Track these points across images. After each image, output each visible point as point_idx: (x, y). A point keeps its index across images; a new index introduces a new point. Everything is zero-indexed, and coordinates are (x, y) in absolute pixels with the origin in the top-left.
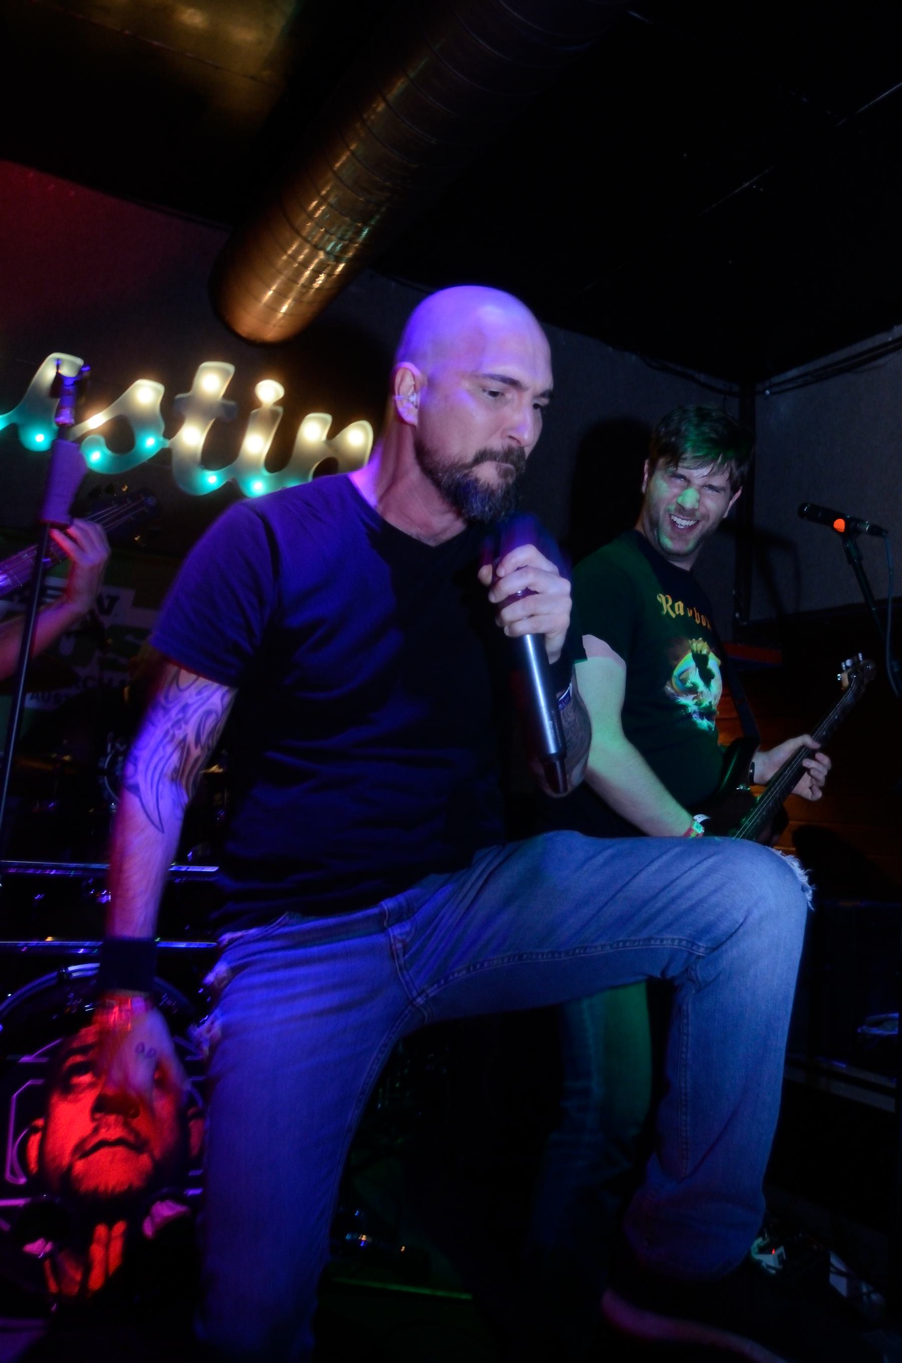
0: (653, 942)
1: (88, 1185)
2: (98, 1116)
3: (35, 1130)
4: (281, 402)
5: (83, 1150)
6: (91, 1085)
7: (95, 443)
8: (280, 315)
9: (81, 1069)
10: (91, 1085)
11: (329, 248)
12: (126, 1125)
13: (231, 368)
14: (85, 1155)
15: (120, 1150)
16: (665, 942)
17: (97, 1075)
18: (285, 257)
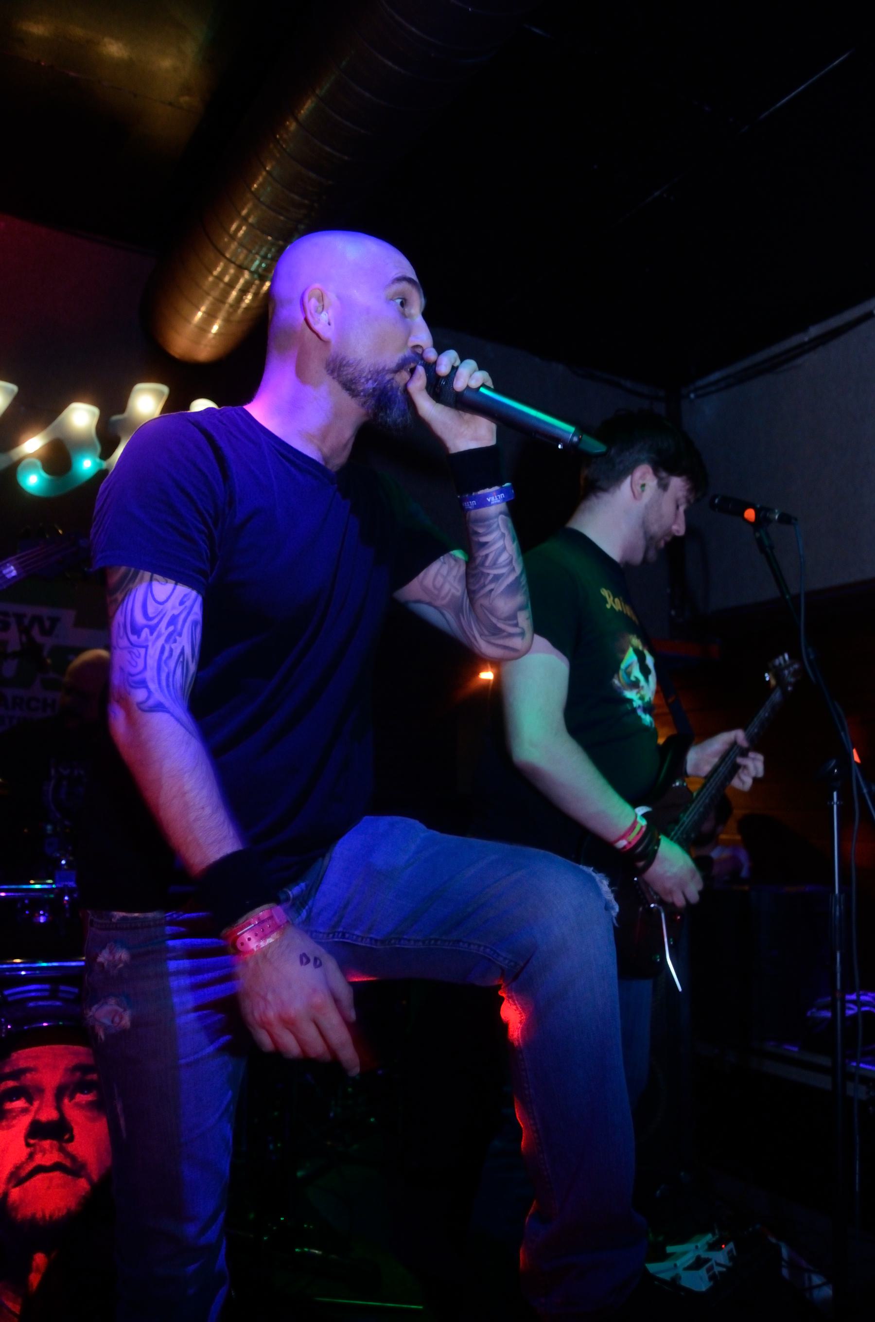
0: (461, 944)
1: (26, 1212)
2: (32, 1142)
6: (25, 1111)
7: (32, 466)
8: (211, 336)
11: (253, 268)
12: (62, 1150)
13: (165, 389)
14: (20, 1182)
15: (56, 1174)
16: (472, 946)
17: (30, 1101)
18: (211, 279)
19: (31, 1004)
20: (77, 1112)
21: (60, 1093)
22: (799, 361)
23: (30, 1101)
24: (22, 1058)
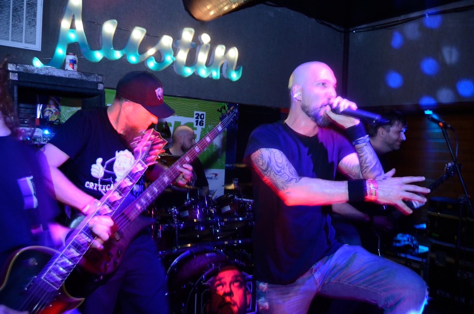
6: (222, 289)
9: (219, 285)
10: (222, 289)
12: (231, 299)
13: (193, 30)
17: (223, 286)
19: (207, 255)
22: (396, 26)
23: (223, 286)
24: (221, 275)
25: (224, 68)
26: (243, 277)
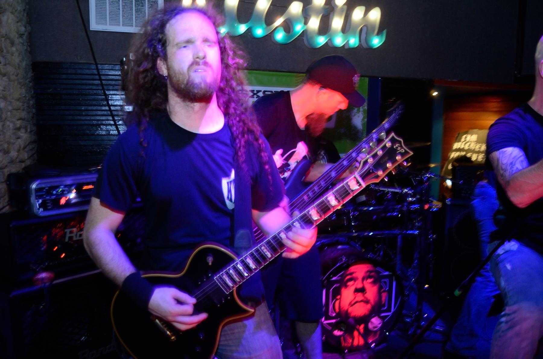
1: (353, 314)
3: (337, 300)
4: (344, 4)
5: (351, 305)
6: (353, 285)
9: (350, 280)
10: (353, 285)
12: (363, 296)
15: (362, 304)
19: (340, 247)
20: (368, 284)
21: (363, 279)
23: (355, 281)
24: (353, 269)
25: (364, 36)
26: (378, 273)
